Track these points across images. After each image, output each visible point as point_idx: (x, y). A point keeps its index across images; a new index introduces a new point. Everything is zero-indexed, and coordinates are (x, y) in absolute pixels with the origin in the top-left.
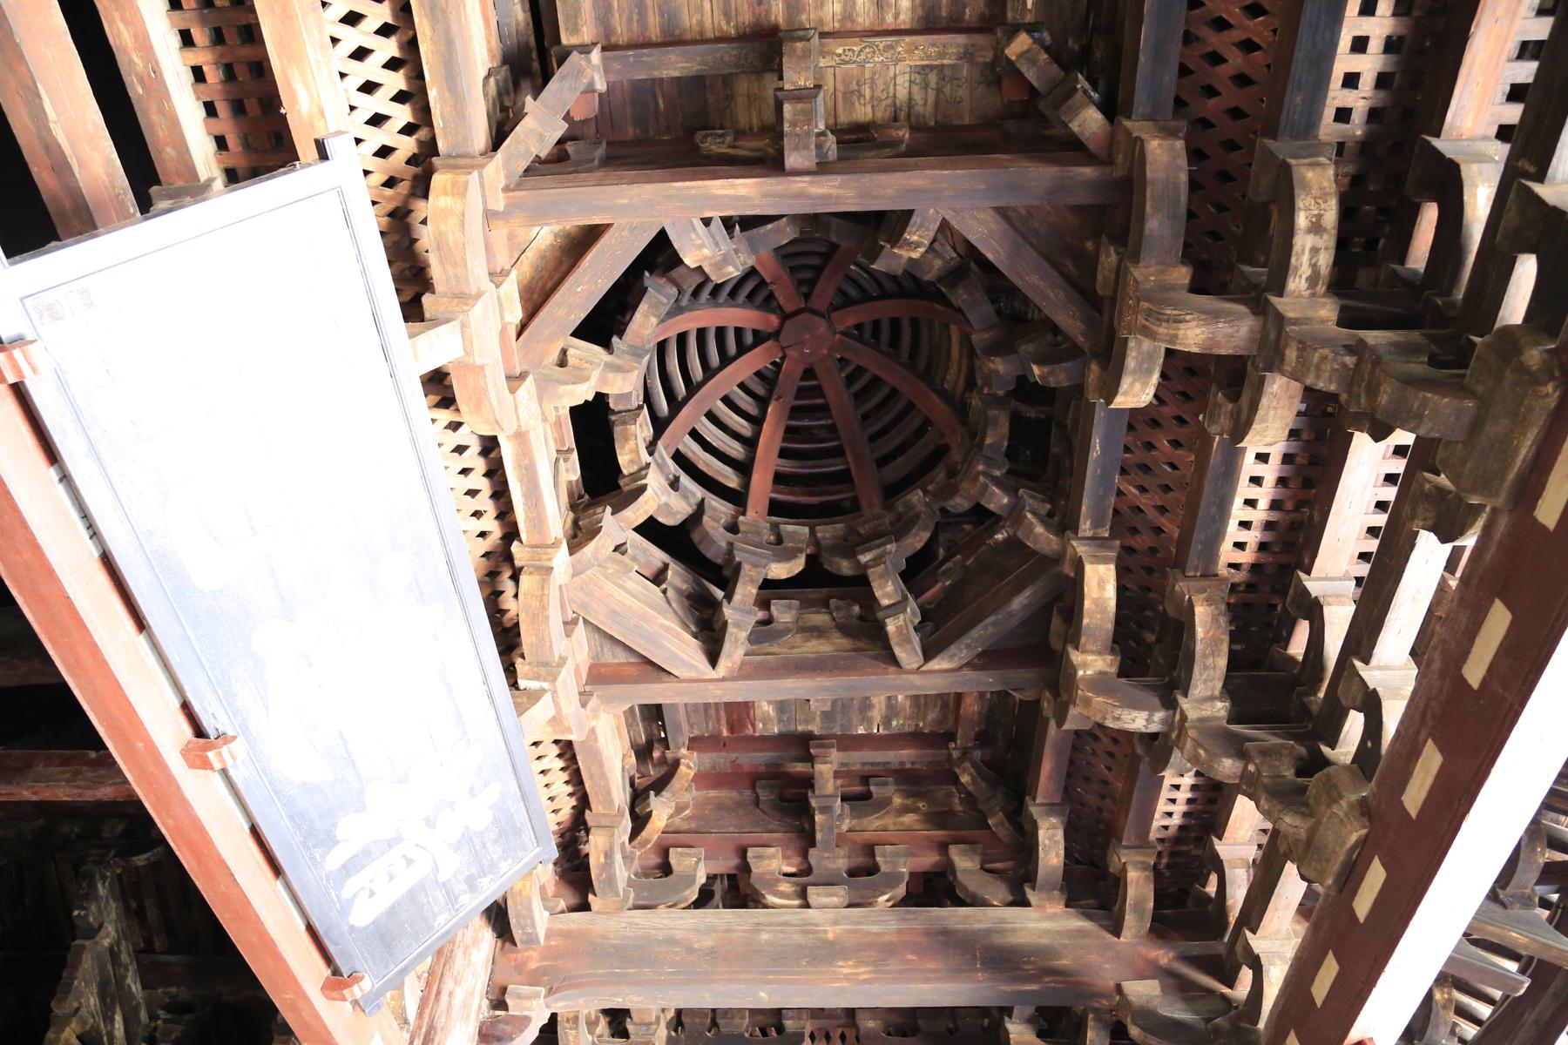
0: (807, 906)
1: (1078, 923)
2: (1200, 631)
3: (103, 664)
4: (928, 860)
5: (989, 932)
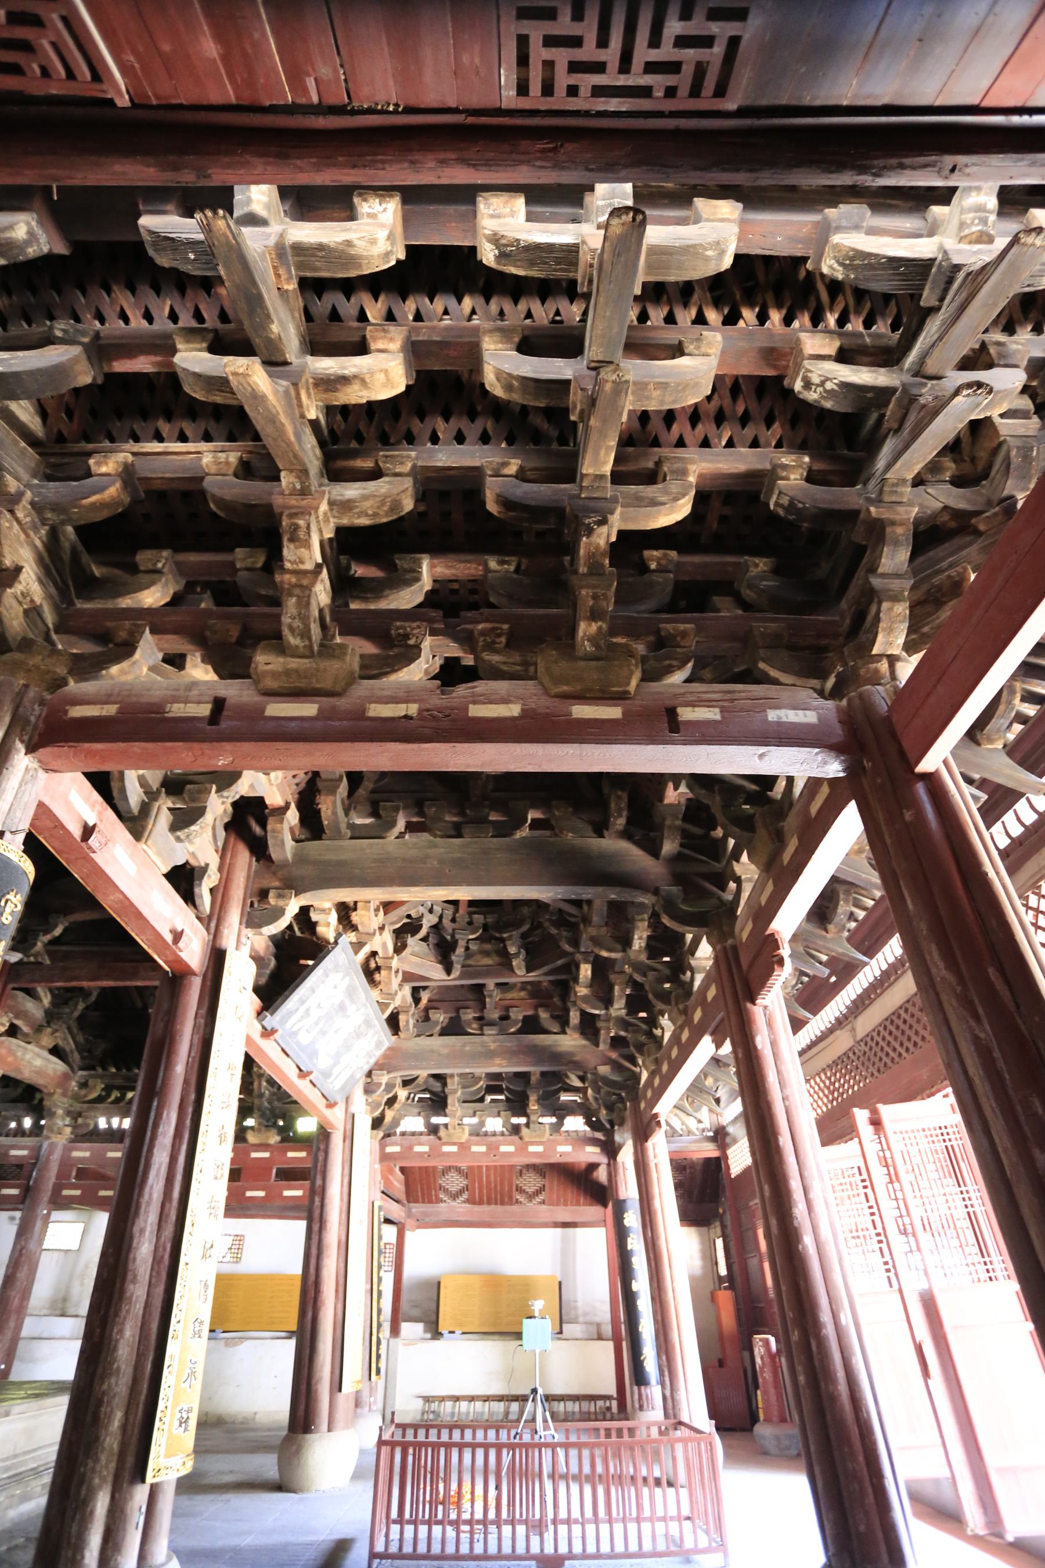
0: (482, 1034)
1: (584, 1042)
2: (616, 994)
3: (265, 1054)
4: (530, 1013)
5: (550, 1046)
